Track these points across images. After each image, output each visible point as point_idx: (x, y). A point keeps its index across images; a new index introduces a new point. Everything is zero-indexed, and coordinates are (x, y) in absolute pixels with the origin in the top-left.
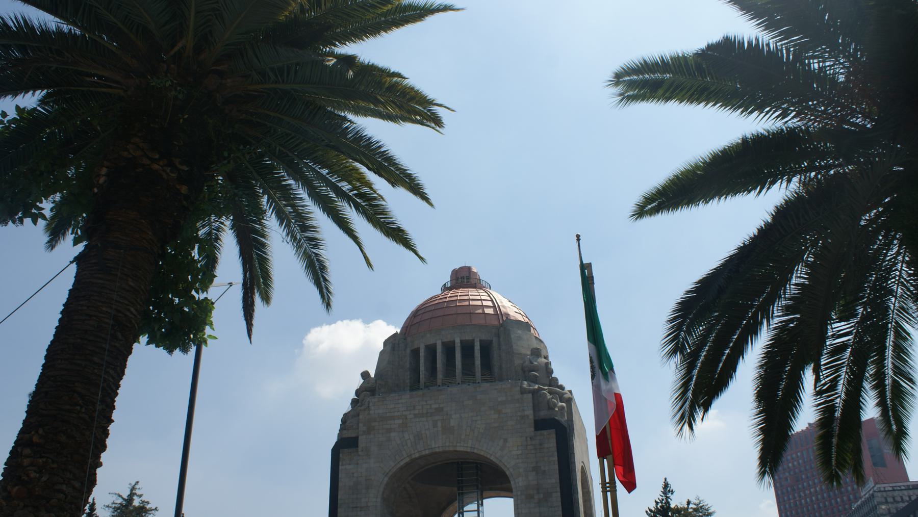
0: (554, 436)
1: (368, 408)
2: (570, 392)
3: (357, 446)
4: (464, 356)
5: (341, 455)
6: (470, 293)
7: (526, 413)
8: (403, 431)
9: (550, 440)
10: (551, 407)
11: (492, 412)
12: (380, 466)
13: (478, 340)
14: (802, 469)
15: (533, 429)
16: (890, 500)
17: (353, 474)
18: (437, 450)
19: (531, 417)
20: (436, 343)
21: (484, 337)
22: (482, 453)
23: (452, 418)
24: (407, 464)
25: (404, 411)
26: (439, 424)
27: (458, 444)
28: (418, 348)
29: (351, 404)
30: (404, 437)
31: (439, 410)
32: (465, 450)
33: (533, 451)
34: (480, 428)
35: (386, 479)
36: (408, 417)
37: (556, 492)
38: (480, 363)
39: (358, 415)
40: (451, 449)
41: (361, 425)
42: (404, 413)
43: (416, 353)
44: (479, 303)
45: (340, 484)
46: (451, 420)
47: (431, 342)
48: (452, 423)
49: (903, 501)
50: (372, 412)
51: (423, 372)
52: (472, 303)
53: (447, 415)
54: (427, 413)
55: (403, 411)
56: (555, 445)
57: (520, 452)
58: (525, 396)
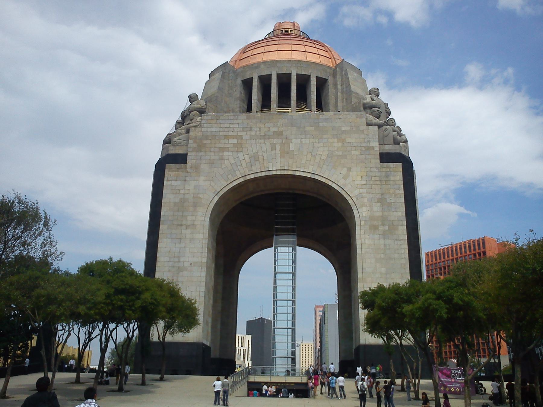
0: (401, 170)
1: (200, 125)
3: (186, 163)
5: (167, 171)
7: (372, 144)
8: (237, 152)
11: (336, 140)
12: (210, 185)
15: (379, 161)
17: (179, 190)
18: (274, 173)
19: (377, 149)
21: (319, 76)
22: (323, 180)
24: (239, 185)
25: (240, 131)
26: (278, 147)
30: (238, 157)
31: (279, 134)
33: (378, 183)
34: (321, 155)
35: (217, 198)
36: (243, 137)
37: (402, 225)
40: (290, 173)
41: (191, 141)
42: (240, 133)
43: (247, 84)
45: (164, 201)
46: (291, 144)
47: (265, 73)
48: (292, 147)
50: (203, 129)
51: (256, 101)
53: (287, 138)
54: (265, 135)
55: (238, 131)
57: (364, 182)
58: (371, 127)
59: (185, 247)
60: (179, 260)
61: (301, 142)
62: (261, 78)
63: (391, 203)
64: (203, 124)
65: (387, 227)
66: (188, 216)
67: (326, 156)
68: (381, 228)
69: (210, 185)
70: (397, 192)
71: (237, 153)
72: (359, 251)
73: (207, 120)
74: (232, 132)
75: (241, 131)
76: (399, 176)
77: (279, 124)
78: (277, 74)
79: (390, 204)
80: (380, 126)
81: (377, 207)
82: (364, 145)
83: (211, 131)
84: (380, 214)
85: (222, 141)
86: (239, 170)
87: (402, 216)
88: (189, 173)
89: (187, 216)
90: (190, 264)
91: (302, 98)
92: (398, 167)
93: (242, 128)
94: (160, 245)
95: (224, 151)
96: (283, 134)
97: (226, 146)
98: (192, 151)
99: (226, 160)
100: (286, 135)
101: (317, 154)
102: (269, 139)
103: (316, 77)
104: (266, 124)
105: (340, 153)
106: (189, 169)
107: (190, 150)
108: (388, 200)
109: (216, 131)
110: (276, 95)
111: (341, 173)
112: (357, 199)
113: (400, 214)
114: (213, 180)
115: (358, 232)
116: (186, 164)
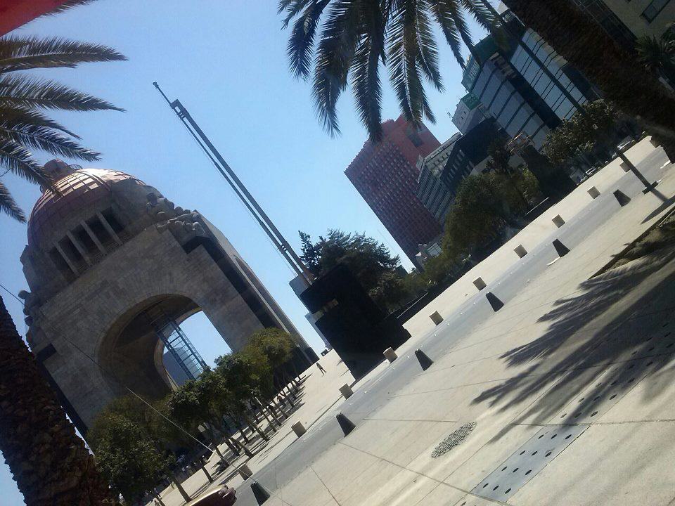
0: (204, 249)
2: (195, 211)
3: (55, 351)
4: (96, 233)
6: (69, 181)
9: (202, 253)
10: (187, 229)
14: (375, 175)
16: (437, 163)
19: (178, 246)
20: (67, 236)
24: (105, 339)
26: (111, 293)
31: (104, 284)
32: (143, 299)
39: (40, 328)
44: (81, 184)
49: (444, 159)
52: (75, 188)
56: (208, 254)
58: (164, 233)
62: (61, 243)
76: (205, 255)
91: (105, 237)
94: (82, 418)
108: (210, 276)
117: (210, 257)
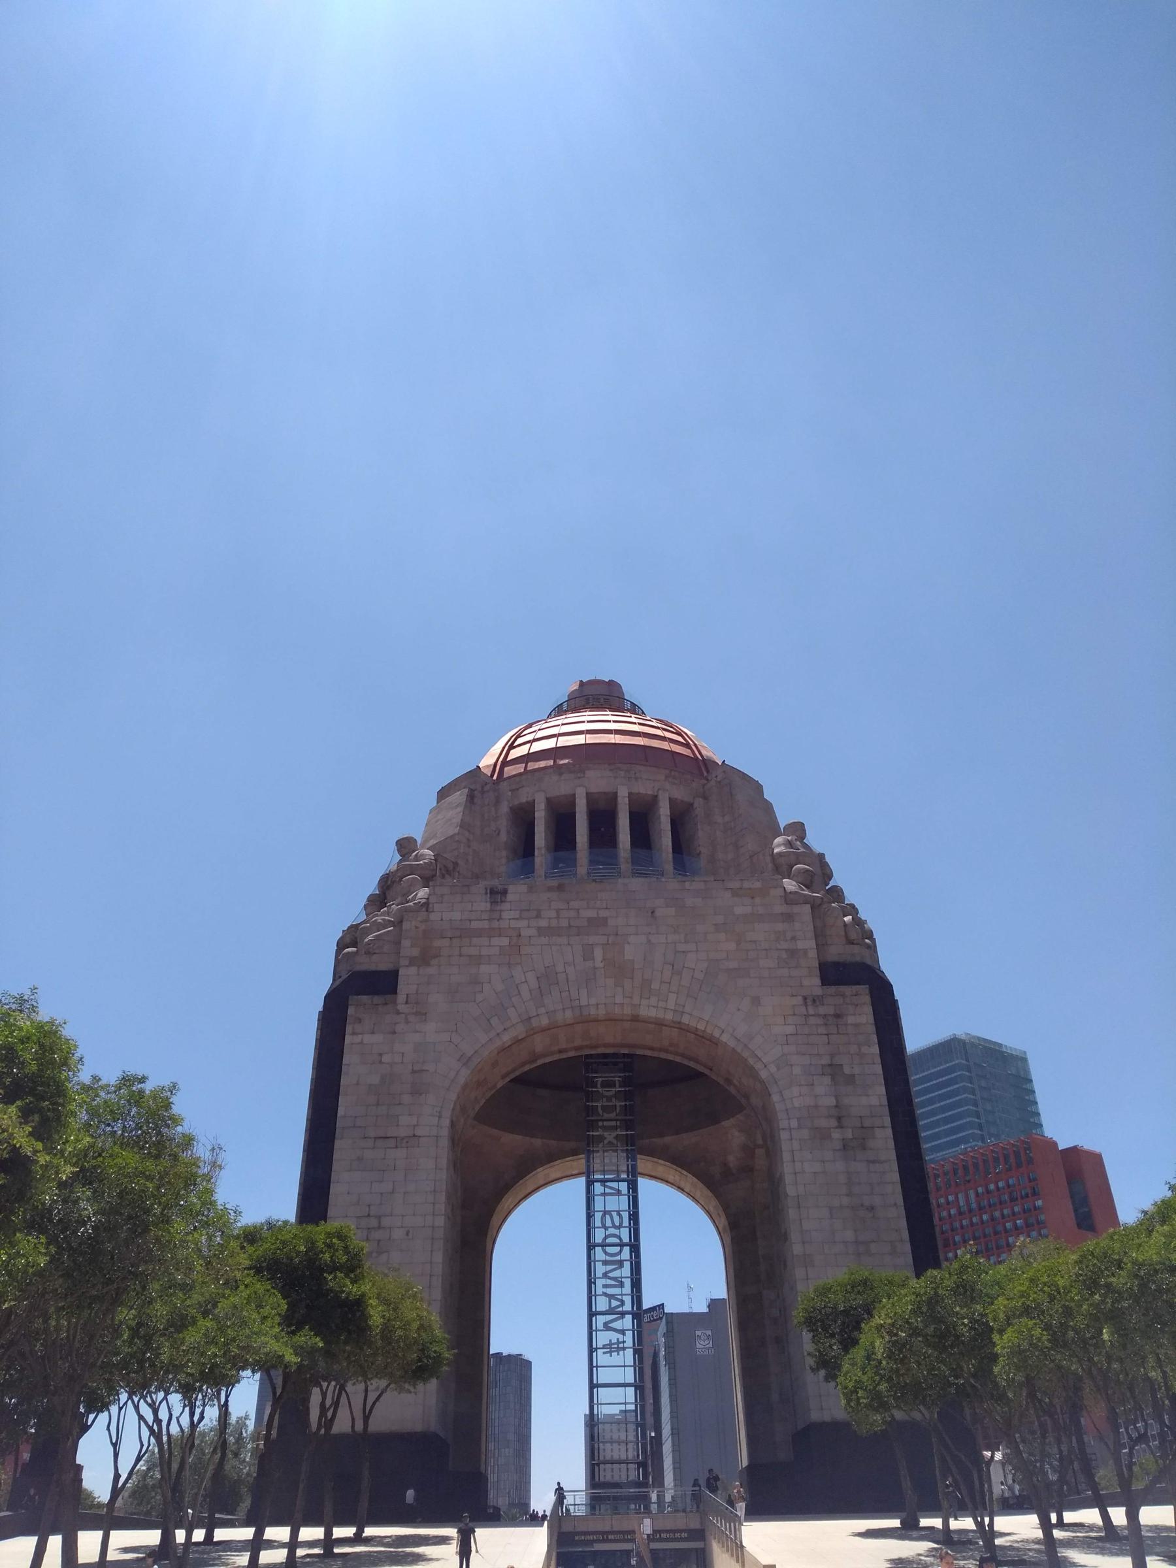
0: (867, 999)
7: (800, 945)
8: (509, 965)
13: (667, 795)
15: (818, 981)
17: (381, 1055)
19: (813, 954)
20: (574, 795)
23: (629, 943)
25: (513, 919)
27: (644, 1002)
28: (527, 802)
29: (365, 907)
31: (598, 923)
32: (661, 1015)
33: (822, 1030)
34: (694, 969)
35: (465, 1075)
36: (522, 934)
37: (883, 1127)
38: (670, 844)
41: (406, 943)
42: (513, 924)
45: (344, 1081)
46: (627, 946)
48: (629, 953)
50: (433, 916)
51: (543, 852)
53: (617, 934)
54: (570, 926)
55: (510, 919)
56: (871, 1019)
57: (790, 1029)
58: (796, 909)
59: (393, 1192)
60: (380, 1223)
61: (649, 941)
63: (854, 1075)
64: (433, 903)
65: (850, 1130)
66: (400, 1117)
67: (704, 971)
68: (836, 1135)
69: (451, 1041)
70: (864, 1049)
71: (509, 967)
72: (791, 1190)
73: (442, 895)
74: (498, 920)
75: (517, 919)
77: (599, 902)
78: (587, 793)
79: (851, 1079)
80: (815, 906)
81: (823, 1086)
82: (785, 945)
83: (451, 920)
84: (831, 1101)
85: (475, 941)
86: (514, 1006)
87: (881, 1105)
88: (403, 1016)
89: (398, 1116)
90: (405, 1233)
92: (862, 995)
93: (518, 912)
95: (479, 964)
96: (611, 922)
97: (484, 952)
98: (411, 964)
99: (484, 984)
100: (617, 927)
101: (684, 967)
102: (578, 935)
103: (670, 798)
104: (572, 903)
105: (733, 965)
106: (403, 1006)
107: (404, 962)
108: (847, 1070)
109: (461, 920)
110: (586, 836)
111: (739, 1010)
112: (778, 1069)
113: (874, 1101)
114: (456, 1031)
115: (785, 1146)
116: (394, 995)
117: (872, 1029)
